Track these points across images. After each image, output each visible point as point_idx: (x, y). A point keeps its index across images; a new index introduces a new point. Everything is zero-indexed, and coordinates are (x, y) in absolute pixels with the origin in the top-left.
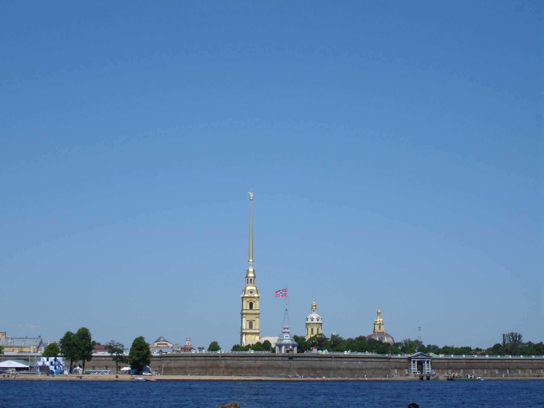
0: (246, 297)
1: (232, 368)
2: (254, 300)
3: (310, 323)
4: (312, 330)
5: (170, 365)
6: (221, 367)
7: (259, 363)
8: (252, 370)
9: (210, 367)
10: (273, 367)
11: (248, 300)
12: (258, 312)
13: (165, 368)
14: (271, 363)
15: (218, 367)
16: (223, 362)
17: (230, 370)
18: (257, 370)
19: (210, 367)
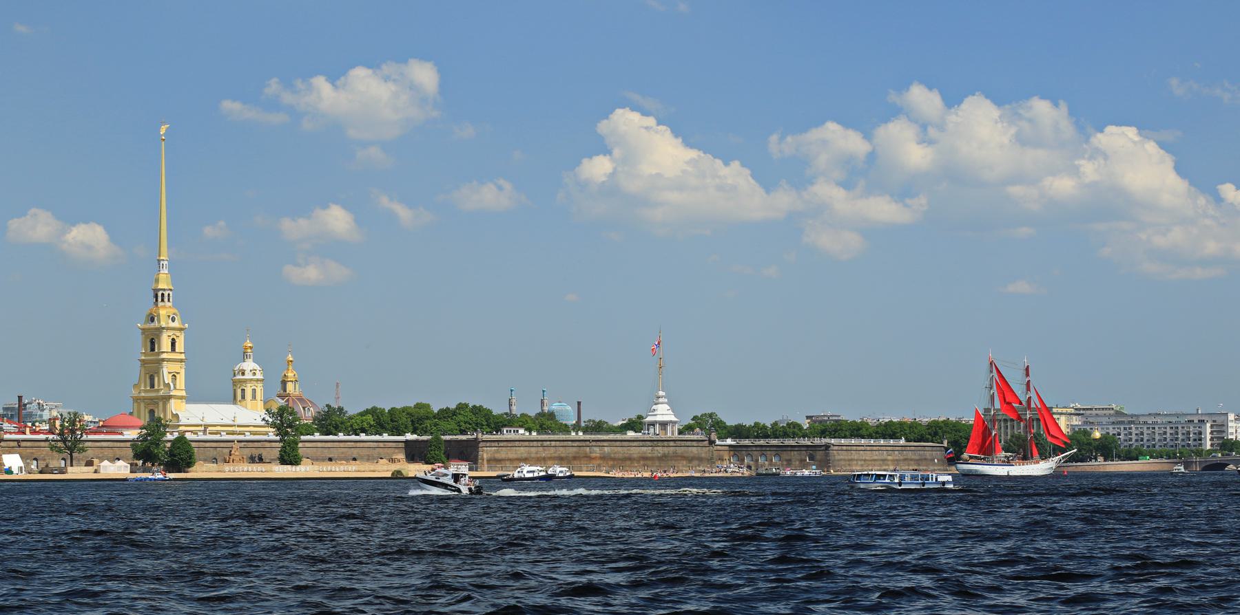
0: (168, 329)
1: (614, 459)
2: (178, 333)
3: (251, 380)
4: (254, 391)
5: (498, 456)
6: (595, 458)
7: (660, 451)
8: (649, 463)
9: (575, 458)
10: (683, 458)
11: (170, 333)
12: (183, 356)
13: (489, 461)
14: (680, 450)
15: (591, 459)
16: (597, 449)
17: (611, 463)
18: (657, 463)
19: (575, 458)
